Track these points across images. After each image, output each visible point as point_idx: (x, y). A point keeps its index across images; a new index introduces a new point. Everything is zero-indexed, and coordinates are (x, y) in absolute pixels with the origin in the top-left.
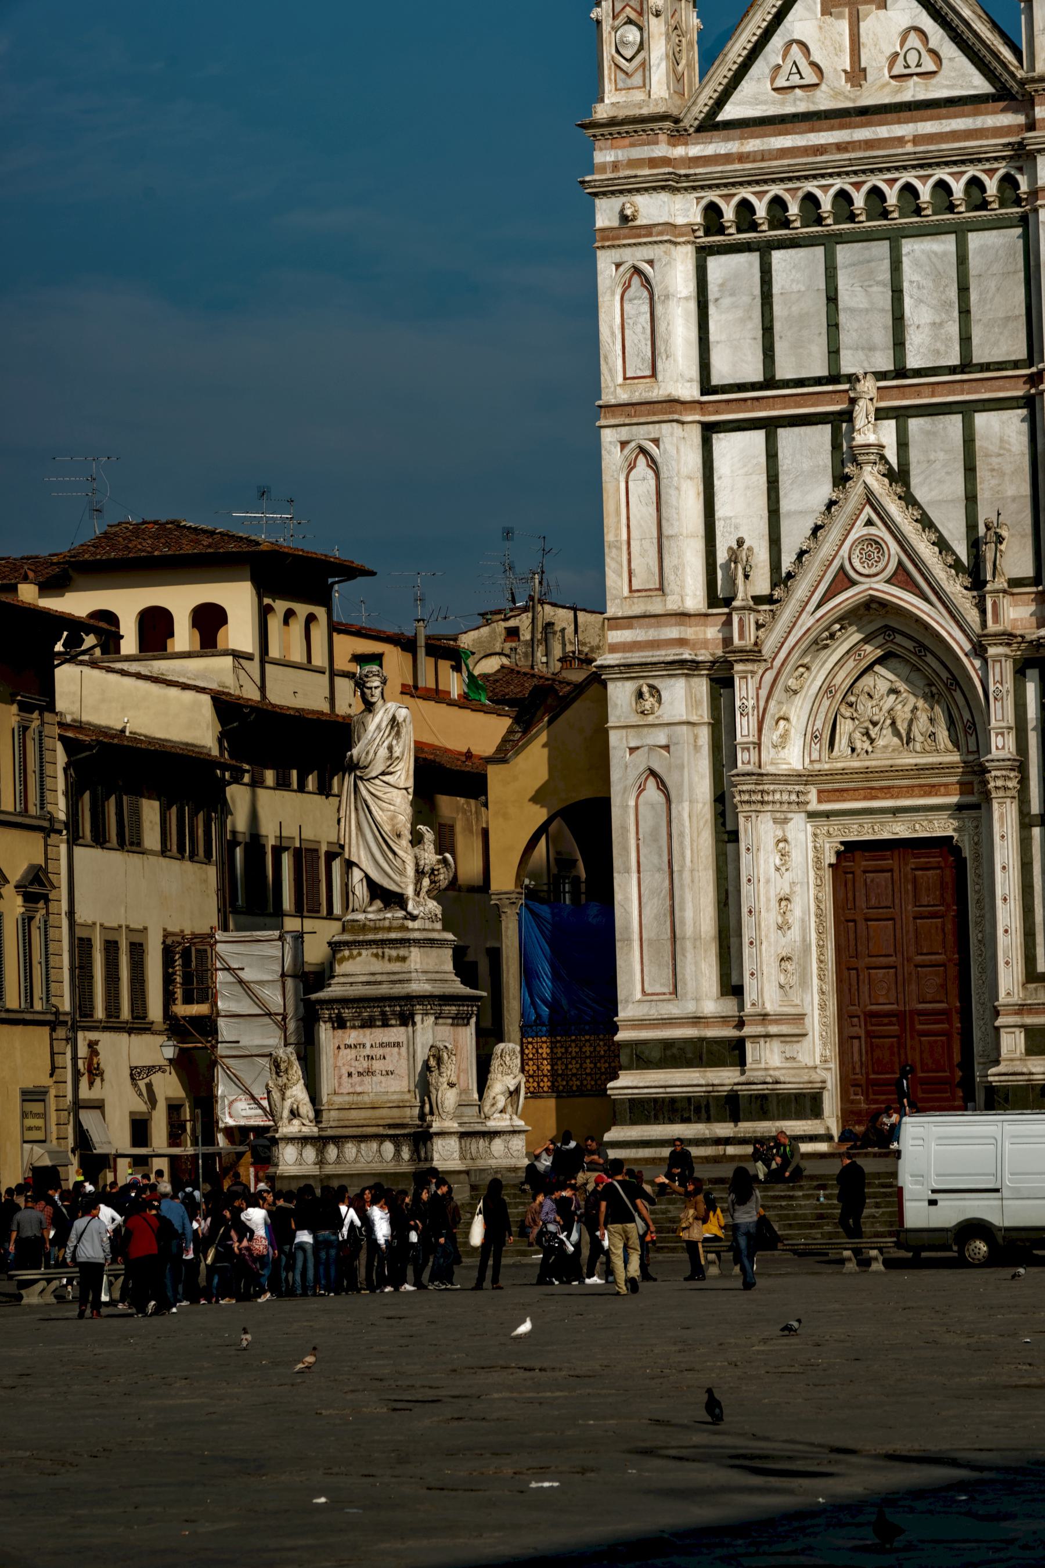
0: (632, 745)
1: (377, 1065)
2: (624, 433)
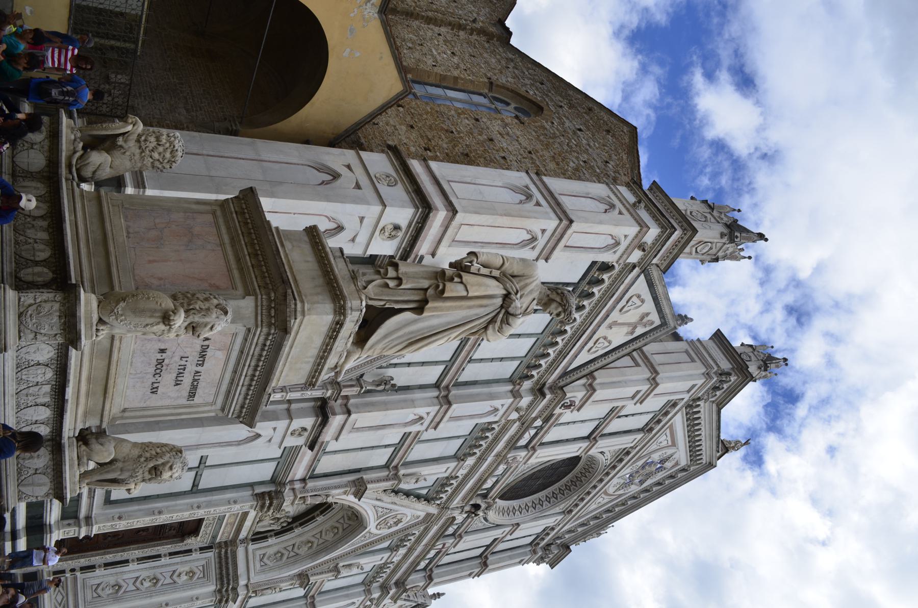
0: (365, 221)
1: (168, 378)
2: (548, 234)
